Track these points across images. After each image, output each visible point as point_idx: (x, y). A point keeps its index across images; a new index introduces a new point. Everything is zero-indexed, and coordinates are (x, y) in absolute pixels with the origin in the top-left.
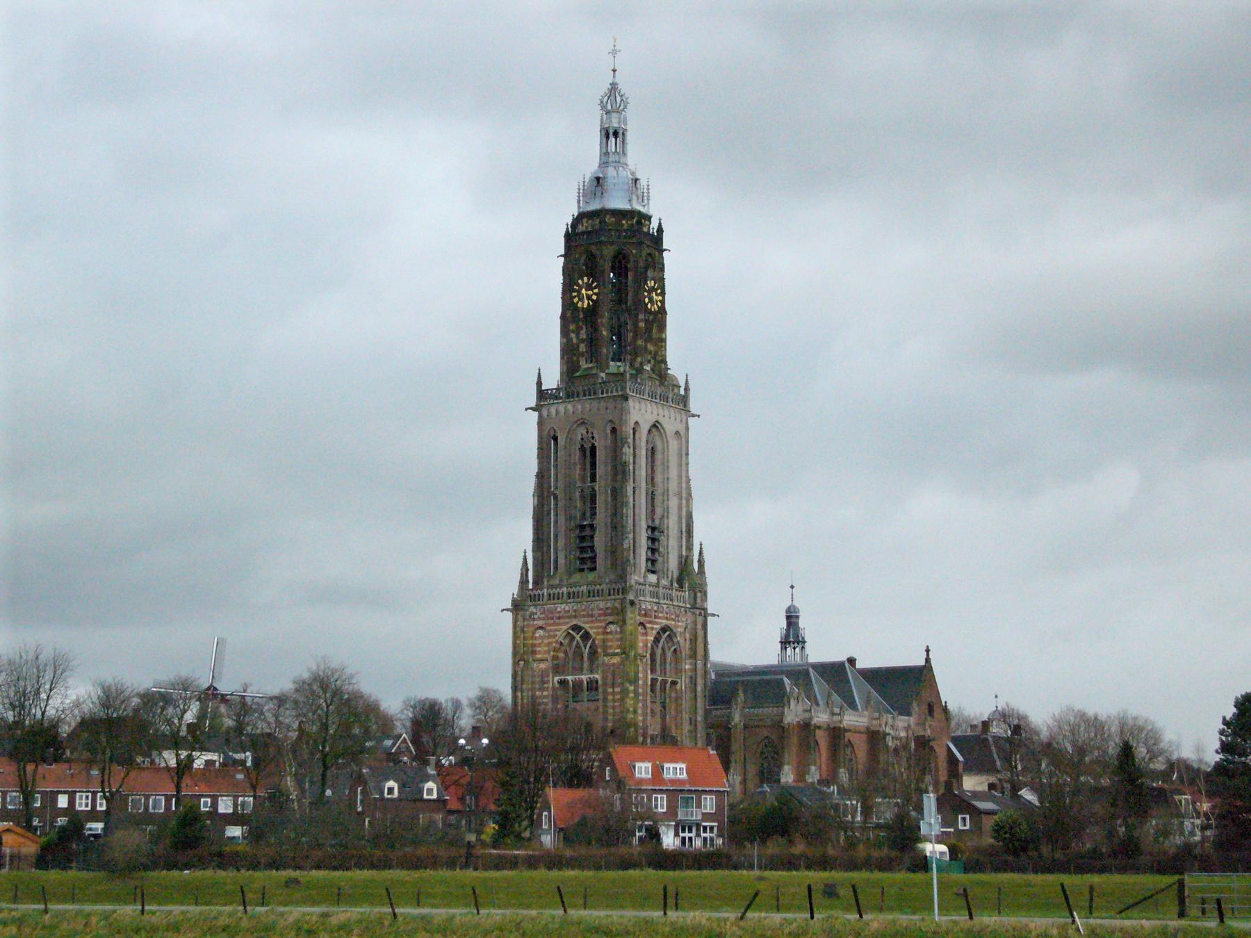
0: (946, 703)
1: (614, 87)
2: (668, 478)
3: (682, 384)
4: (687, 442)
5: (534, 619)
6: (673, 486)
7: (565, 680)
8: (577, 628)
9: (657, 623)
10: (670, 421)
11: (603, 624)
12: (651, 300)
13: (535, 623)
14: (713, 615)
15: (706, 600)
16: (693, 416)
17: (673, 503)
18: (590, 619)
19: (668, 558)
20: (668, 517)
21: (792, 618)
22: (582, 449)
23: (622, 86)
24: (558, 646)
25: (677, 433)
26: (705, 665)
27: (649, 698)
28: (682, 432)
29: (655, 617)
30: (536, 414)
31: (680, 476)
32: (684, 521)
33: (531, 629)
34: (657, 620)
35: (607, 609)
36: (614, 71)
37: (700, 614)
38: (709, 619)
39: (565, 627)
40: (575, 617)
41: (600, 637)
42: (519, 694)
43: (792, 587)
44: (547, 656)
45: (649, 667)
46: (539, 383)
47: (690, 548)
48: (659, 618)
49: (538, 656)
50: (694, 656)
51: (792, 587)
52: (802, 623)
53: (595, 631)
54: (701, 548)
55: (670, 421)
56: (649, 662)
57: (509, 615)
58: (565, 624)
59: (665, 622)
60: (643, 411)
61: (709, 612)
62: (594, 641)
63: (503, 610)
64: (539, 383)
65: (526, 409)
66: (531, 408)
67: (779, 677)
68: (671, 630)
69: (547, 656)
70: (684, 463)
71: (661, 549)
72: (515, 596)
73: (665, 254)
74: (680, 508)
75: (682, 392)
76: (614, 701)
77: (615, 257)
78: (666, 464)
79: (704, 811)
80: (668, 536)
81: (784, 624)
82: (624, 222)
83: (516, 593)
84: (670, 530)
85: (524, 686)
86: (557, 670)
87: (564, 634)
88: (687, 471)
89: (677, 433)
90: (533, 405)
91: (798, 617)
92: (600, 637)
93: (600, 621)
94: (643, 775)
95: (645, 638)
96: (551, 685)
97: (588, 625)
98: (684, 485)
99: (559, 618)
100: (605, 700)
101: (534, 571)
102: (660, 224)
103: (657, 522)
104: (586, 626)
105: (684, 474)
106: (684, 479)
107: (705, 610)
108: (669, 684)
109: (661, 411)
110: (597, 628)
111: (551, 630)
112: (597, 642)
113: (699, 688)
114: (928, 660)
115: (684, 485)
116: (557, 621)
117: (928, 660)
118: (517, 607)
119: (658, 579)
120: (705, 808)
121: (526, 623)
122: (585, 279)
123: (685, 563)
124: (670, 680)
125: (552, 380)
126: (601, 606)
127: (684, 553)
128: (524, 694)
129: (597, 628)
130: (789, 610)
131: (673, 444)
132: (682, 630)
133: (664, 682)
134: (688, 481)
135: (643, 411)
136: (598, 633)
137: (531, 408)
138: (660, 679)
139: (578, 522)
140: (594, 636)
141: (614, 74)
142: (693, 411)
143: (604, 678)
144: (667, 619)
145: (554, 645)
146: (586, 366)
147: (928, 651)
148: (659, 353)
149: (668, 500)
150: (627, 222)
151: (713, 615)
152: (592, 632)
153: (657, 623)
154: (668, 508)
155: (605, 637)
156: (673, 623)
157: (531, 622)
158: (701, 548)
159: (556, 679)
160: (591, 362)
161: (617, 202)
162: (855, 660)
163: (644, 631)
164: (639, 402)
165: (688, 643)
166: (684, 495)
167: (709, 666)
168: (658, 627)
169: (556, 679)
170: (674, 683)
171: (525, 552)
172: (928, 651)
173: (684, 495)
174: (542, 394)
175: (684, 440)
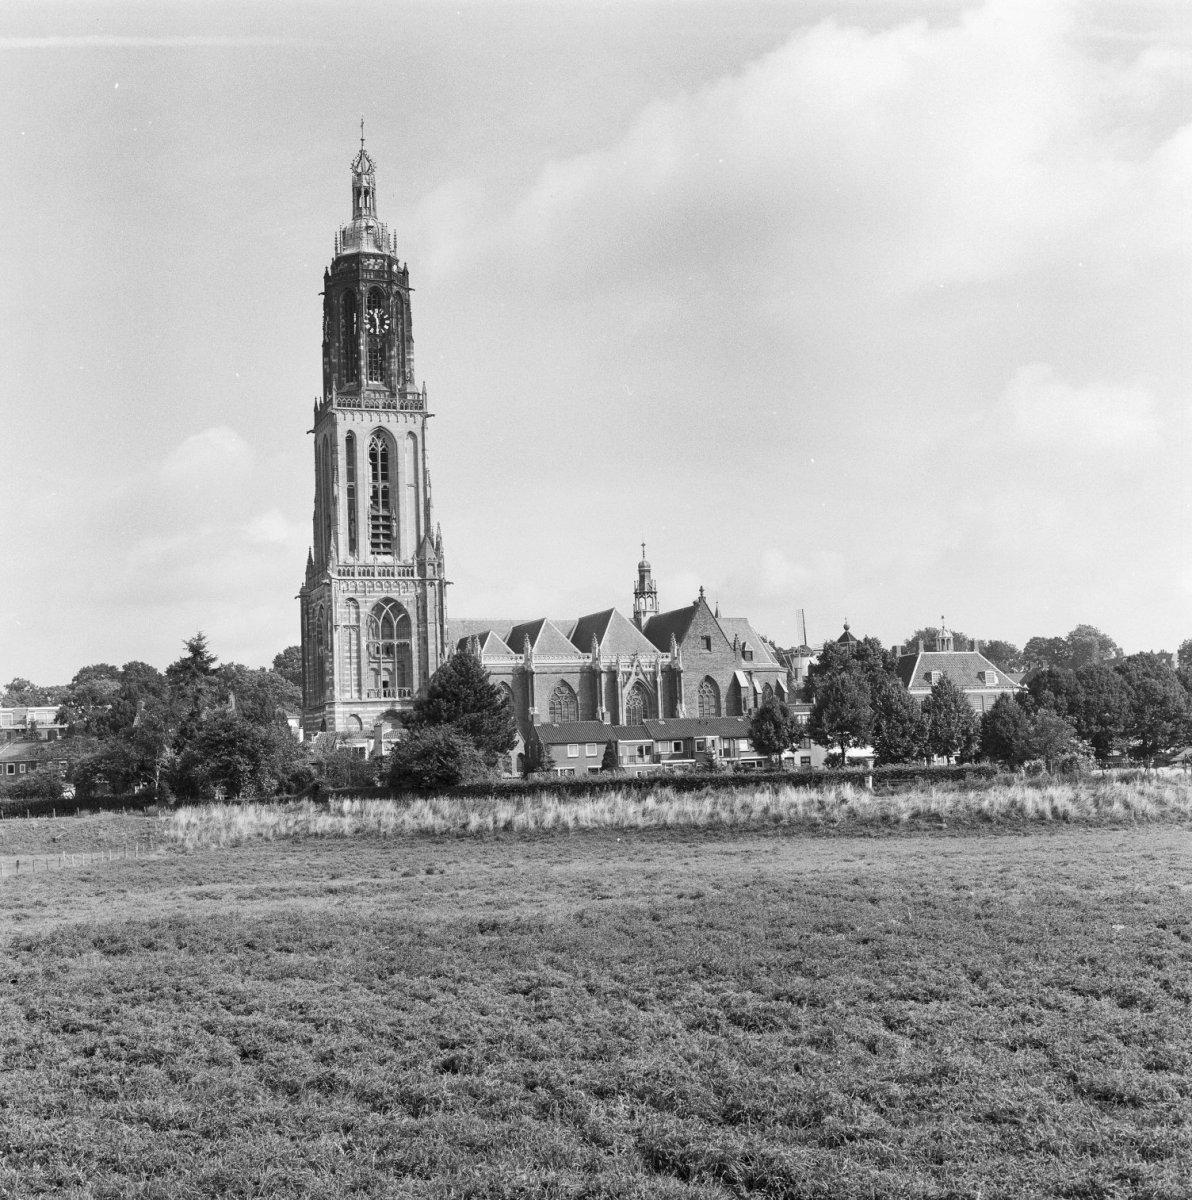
1: (362, 153)
10: (399, 425)
16: (428, 416)
21: (643, 571)
30: (313, 435)
43: (643, 545)
51: (643, 545)
55: (399, 425)
59: (384, 595)
83: (304, 581)
89: (411, 433)
98: (421, 476)
109: (384, 417)
114: (702, 598)
130: (641, 566)
134: (425, 472)
147: (701, 590)
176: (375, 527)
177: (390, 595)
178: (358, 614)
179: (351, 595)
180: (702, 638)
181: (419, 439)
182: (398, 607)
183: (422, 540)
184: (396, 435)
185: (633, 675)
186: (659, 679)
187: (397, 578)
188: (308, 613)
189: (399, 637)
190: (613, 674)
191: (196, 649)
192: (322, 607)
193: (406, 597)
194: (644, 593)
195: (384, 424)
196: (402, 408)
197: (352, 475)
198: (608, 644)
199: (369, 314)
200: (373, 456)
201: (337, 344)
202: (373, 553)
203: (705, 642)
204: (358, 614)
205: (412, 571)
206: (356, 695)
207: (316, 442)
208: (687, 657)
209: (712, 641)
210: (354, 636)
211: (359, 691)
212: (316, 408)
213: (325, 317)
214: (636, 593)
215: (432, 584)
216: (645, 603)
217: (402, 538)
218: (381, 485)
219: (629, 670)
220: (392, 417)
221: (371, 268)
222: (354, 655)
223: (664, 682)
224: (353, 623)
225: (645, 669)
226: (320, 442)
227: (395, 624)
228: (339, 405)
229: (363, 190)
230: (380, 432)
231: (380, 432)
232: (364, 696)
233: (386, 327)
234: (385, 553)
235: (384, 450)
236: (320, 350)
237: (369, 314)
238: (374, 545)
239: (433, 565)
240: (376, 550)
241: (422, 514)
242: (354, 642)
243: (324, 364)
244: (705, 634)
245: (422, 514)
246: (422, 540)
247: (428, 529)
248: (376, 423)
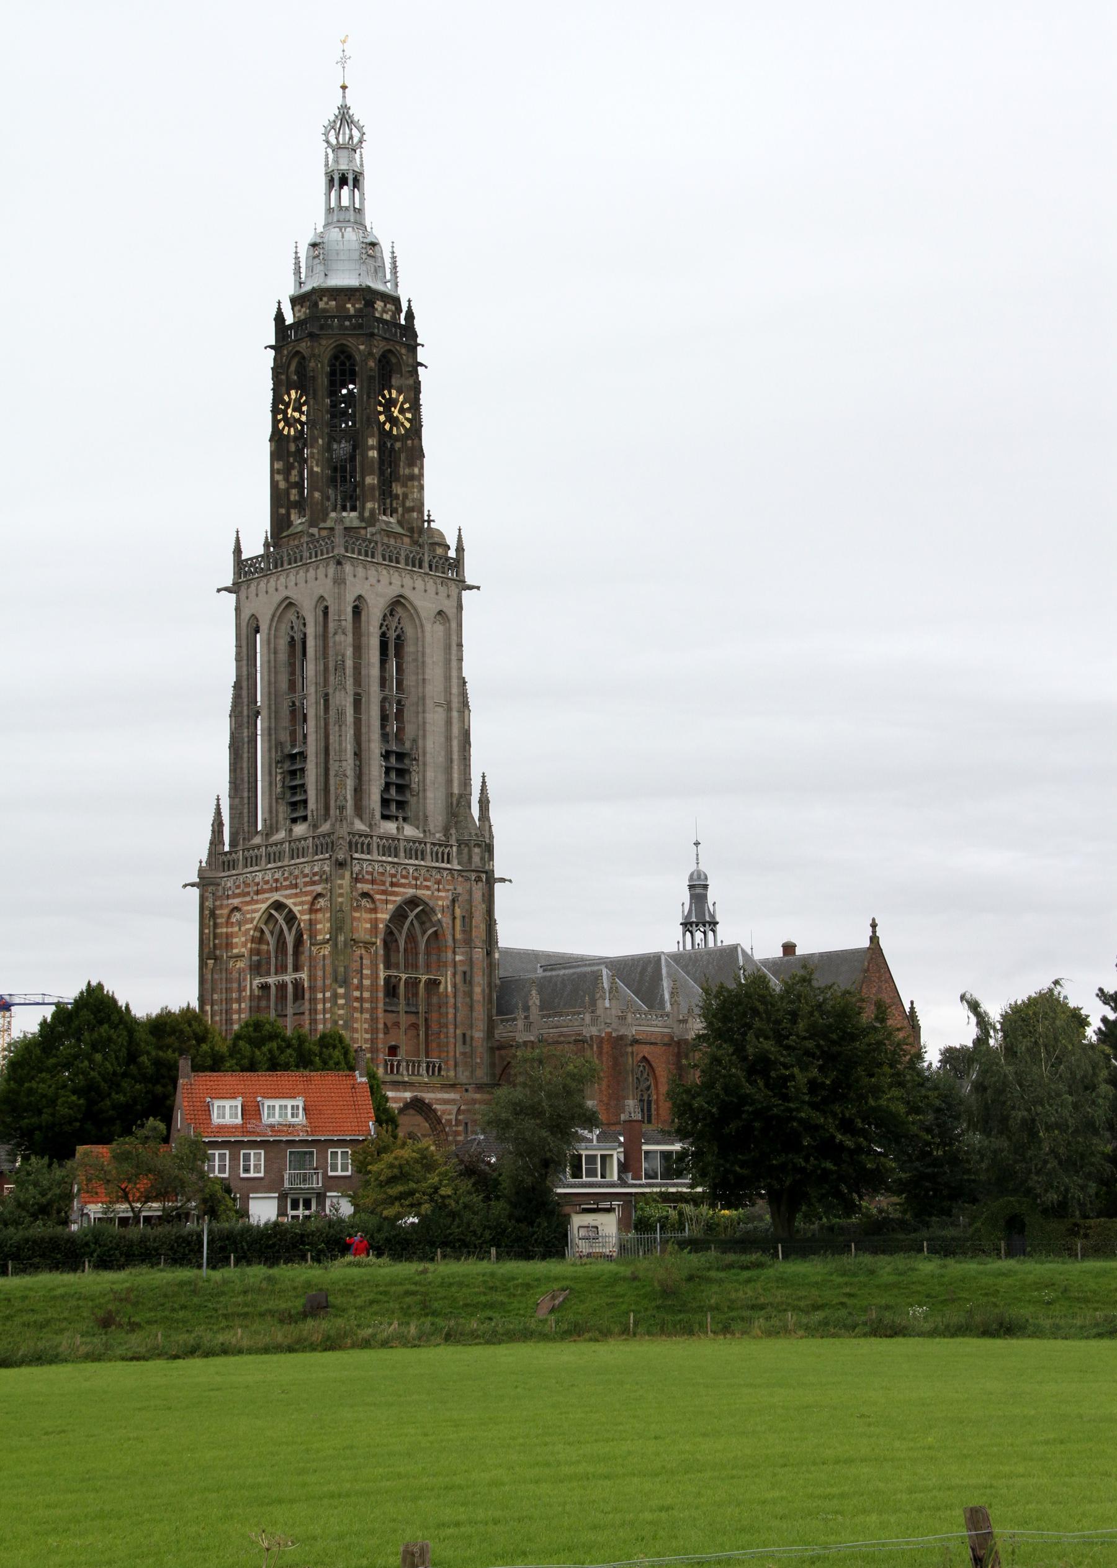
0: (912, 1003)
2: (424, 680)
3: (453, 545)
4: (460, 625)
5: (228, 897)
6: (434, 689)
7: (266, 983)
8: (278, 906)
11: (309, 898)
12: (394, 421)
13: (230, 901)
14: (503, 880)
15: (491, 858)
16: (470, 588)
17: (435, 718)
18: (294, 891)
19: (425, 798)
20: (424, 736)
21: (698, 890)
22: (292, 642)
23: (356, 112)
24: (257, 934)
25: (440, 613)
26: (489, 954)
27: (381, 1005)
28: (451, 612)
29: (392, 884)
30: (234, 595)
31: (448, 678)
32: (455, 743)
33: (225, 911)
34: (396, 889)
35: (315, 874)
36: (344, 88)
37: (478, 880)
39: (264, 906)
40: (277, 889)
41: (307, 917)
42: (208, 1008)
43: (697, 844)
44: (243, 950)
45: (381, 959)
46: (238, 551)
47: (466, 782)
48: (403, 885)
49: (235, 951)
50: (468, 942)
51: (697, 844)
52: (712, 896)
53: (300, 908)
54: (484, 782)
56: (381, 952)
57: (195, 892)
58: (263, 902)
59: (411, 892)
60: (372, 580)
61: (496, 876)
62: (299, 925)
63: (185, 886)
64: (238, 551)
65: (219, 590)
66: (226, 589)
67: (595, 968)
68: (427, 904)
69: (243, 950)
70: (454, 658)
71: (413, 786)
72: (204, 864)
73: (419, 348)
74: (449, 722)
75: (452, 554)
76: (324, 1011)
77: (335, 357)
78: (420, 660)
79: (330, 1174)
80: (424, 764)
81: (686, 896)
82: (349, 306)
83: (204, 858)
84: (428, 755)
85: (216, 997)
86: (257, 969)
87: (265, 917)
88: (460, 669)
90: (229, 582)
91: (706, 887)
92: (307, 917)
93: (306, 894)
94: (228, 1120)
95: (373, 916)
96: (248, 994)
97: (292, 901)
98: (455, 691)
99: (257, 893)
100: (313, 1011)
101: (231, 827)
102: (409, 307)
103: (408, 745)
104: (289, 902)
105: (454, 674)
106: (455, 681)
107: (490, 874)
108: (422, 985)
109: (408, 581)
110: (302, 903)
111: (248, 912)
112: (302, 925)
113: (477, 990)
114: (874, 939)
115: (455, 691)
116: (255, 897)
117: (874, 939)
118: (206, 883)
119: (398, 828)
120: (334, 1169)
121: (218, 903)
122: (293, 393)
123: (457, 805)
124: (424, 978)
125: (253, 548)
126: (307, 871)
127: (456, 791)
128: (216, 1007)
129: (302, 903)
131: (433, 633)
132: (446, 903)
133: (413, 984)
135: (372, 580)
136: (302, 912)
137: (226, 589)
138: (404, 976)
139: (287, 750)
140: (298, 916)
141: (344, 93)
142: (469, 581)
143: (312, 977)
144: (416, 887)
145: (252, 932)
146: (299, 521)
147: (874, 926)
148: (410, 496)
149: (424, 712)
150: (353, 306)
151: (503, 880)
152: (296, 909)
154: (424, 723)
155: (313, 917)
156: (429, 893)
157: (225, 902)
158: (484, 782)
159: (256, 982)
160: (304, 516)
161: (345, 278)
162: (795, 946)
163: (372, 906)
164: (365, 568)
165: (458, 922)
166: (455, 705)
167: (497, 956)
168: (398, 899)
169: (257, 982)
170: (433, 984)
171: (218, 799)
172: (874, 926)
173: (455, 705)
174: (241, 565)
175: (454, 625)
176: (388, 771)
184: (423, 614)
188: (213, 914)
195: (407, 592)
220: (419, 584)
231: (397, 604)
241: (455, 756)
245: (455, 756)
248: (393, 591)
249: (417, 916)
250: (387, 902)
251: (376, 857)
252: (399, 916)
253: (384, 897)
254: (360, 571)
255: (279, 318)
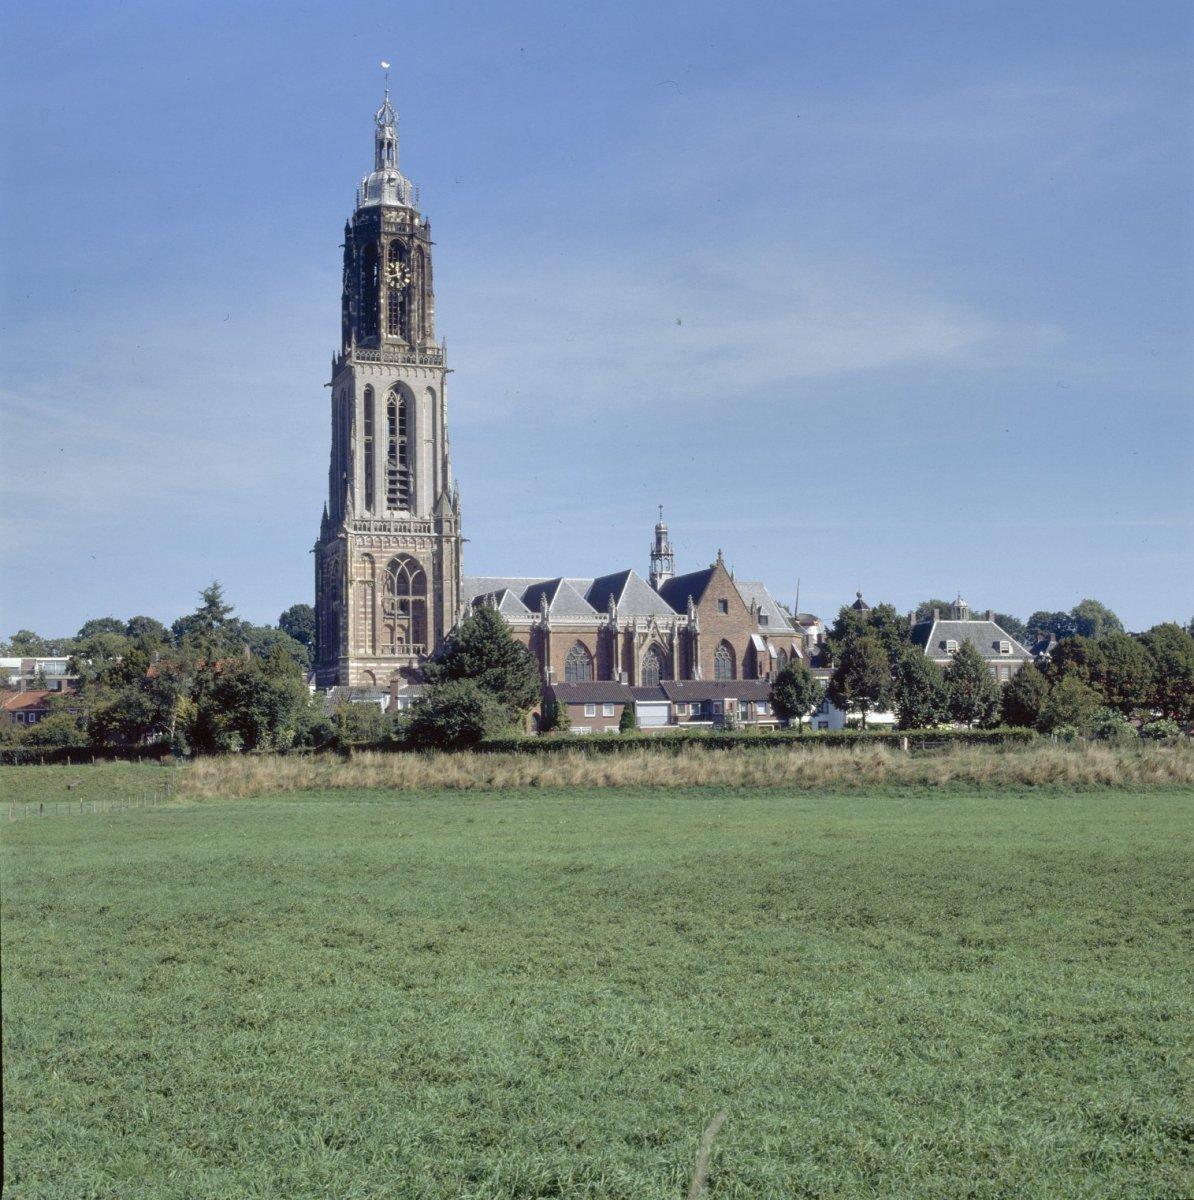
9: (390, 552)
16: (448, 371)
28: (437, 387)
30: (331, 388)
38: (464, 546)
43: (661, 507)
51: (661, 507)
55: (417, 380)
59: (400, 551)
85: (324, 612)
89: (430, 389)
90: (329, 381)
98: (439, 432)
109: (402, 371)
114: (719, 561)
130: (658, 528)
147: (720, 554)
151: (465, 540)
153: (390, 552)
172: (720, 554)
176: (392, 482)
177: (406, 551)
178: (373, 569)
179: (367, 550)
180: (720, 601)
181: (438, 394)
182: (413, 564)
183: (439, 496)
184: (415, 391)
185: (650, 637)
186: (676, 641)
187: (413, 534)
188: (322, 568)
189: (414, 594)
190: (629, 636)
191: (212, 601)
192: (337, 562)
193: (421, 553)
194: (661, 555)
195: (403, 378)
196: (421, 362)
197: (369, 429)
198: (624, 604)
199: (390, 267)
200: (391, 411)
201: (357, 297)
202: (389, 508)
203: (722, 605)
204: (373, 569)
205: (429, 527)
206: (370, 651)
207: (333, 396)
208: (701, 617)
209: (729, 605)
210: (369, 591)
211: (374, 647)
212: (334, 361)
213: (345, 270)
214: (652, 555)
215: (448, 541)
216: (661, 566)
217: (419, 494)
218: (398, 439)
219: (646, 631)
220: (411, 372)
221: (392, 220)
222: (369, 610)
223: (680, 644)
224: (368, 578)
225: (661, 631)
226: (338, 396)
227: (411, 580)
228: (358, 358)
229: (386, 142)
230: (399, 387)
231: (399, 387)
232: (378, 652)
233: (407, 281)
234: (402, 509)
235: (402, 404)
236: (340, 304)
237: (390, 267)
238: (391, 500)
239: (450, 522)
240: (392, 505)
242: (369, 597)
243: (344, 316)
244: (721, 597)
246: (439, 496)
247: (445, 486)
249: (406, 564)
250: (382, 557)
251: (373, 532)
252: (393, 565)
253: (379, 555)
254: (367, 368)
255: (348, 225)
